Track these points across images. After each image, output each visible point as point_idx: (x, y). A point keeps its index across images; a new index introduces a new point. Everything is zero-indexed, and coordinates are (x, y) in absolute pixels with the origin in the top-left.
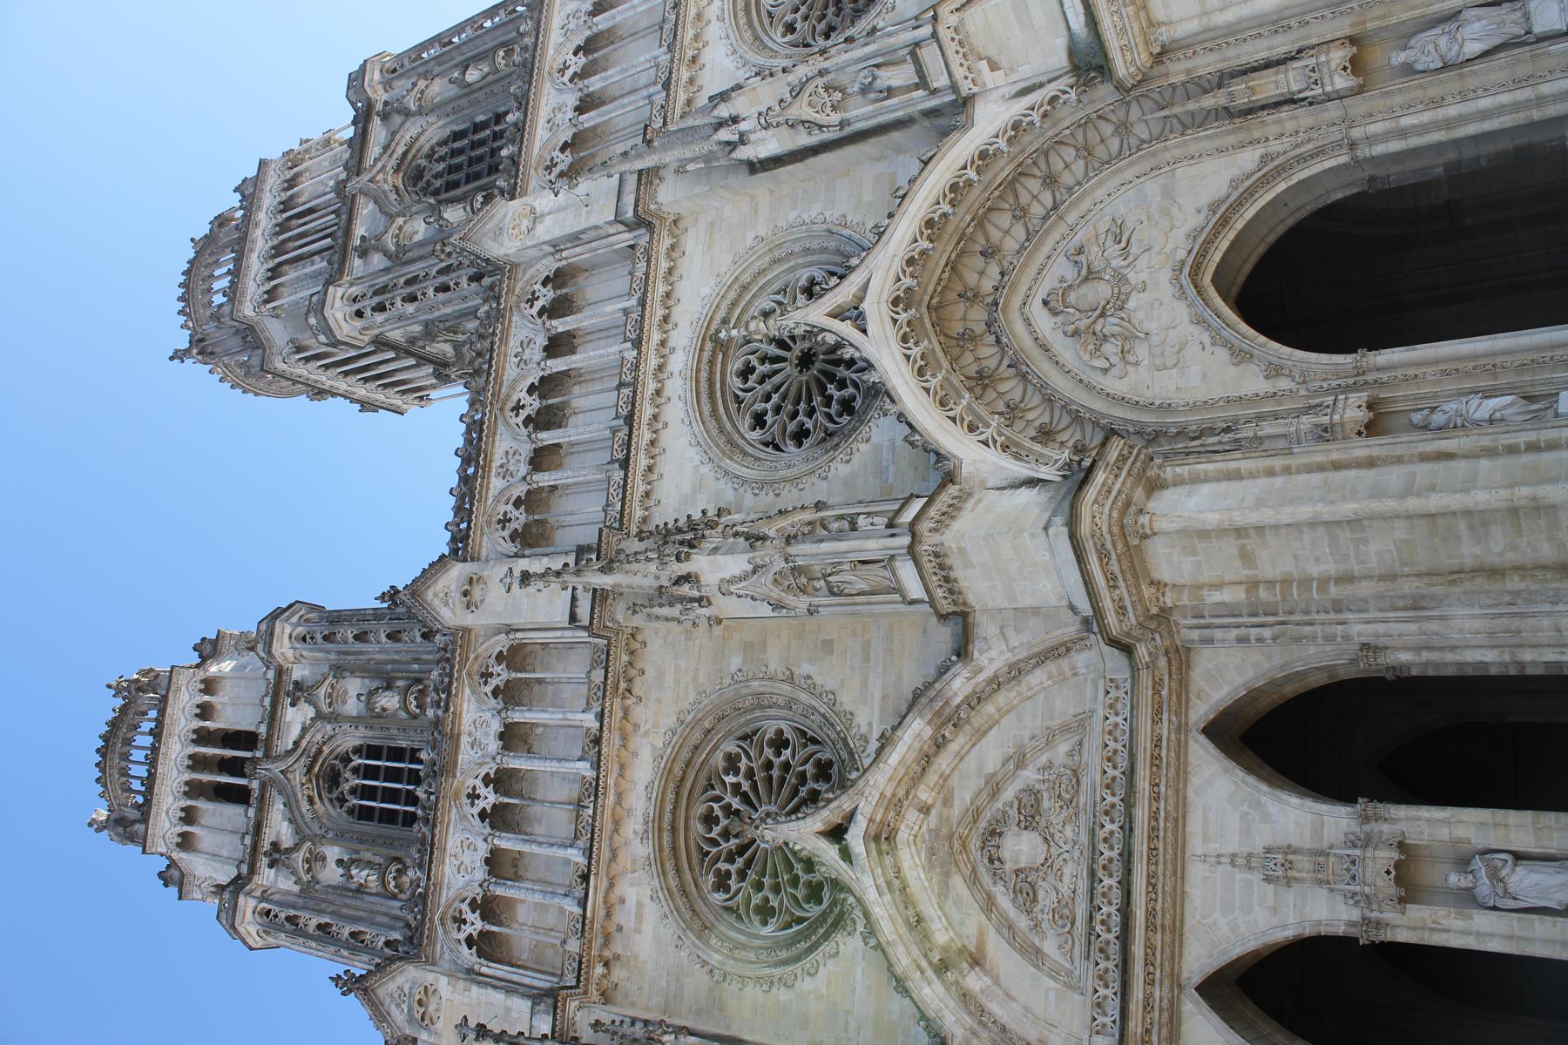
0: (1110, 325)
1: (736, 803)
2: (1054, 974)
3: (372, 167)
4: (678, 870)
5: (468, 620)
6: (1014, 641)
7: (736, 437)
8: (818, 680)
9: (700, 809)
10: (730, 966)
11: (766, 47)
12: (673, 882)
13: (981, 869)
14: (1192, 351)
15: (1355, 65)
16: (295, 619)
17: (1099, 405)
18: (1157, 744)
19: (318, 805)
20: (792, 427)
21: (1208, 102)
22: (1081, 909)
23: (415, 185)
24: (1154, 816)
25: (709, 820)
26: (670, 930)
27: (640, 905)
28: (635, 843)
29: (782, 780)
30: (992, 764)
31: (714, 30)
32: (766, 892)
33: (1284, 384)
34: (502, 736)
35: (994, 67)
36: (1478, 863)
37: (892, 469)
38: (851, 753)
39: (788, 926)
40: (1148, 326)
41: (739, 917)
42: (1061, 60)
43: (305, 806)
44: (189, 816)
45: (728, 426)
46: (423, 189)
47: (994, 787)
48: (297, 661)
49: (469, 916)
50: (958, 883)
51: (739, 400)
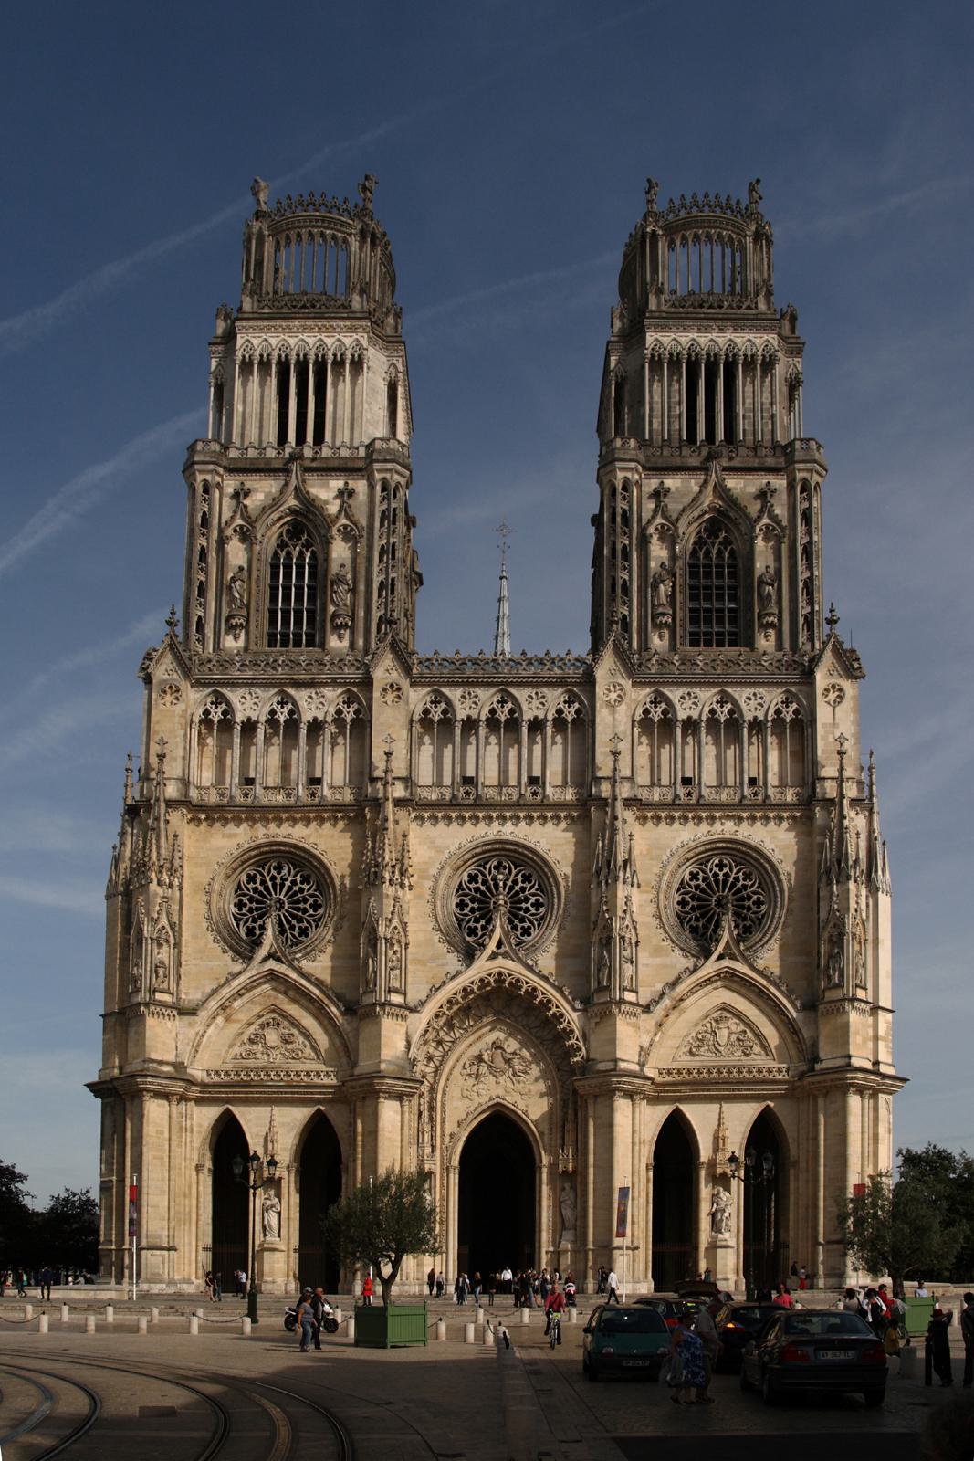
0: (484, 1069)
1: (288, 883)
2: (227, 1052)
6: (350, 1035)
7: (463, 868)
8: (341, 932)
10: (215, 895)
12: (246, 856)
13: (263, 1019)
15: (565, 1172)
16: (397, 477)
17: (450, 1063)
18: (312, 1093)
21: (570, 1112)
22: (251, 1063)
24: (286, 1093)
26: (227, 860)
27: (235, 835)
28: (263, 833)
31: (704, 827)
32: (249, 905)
34: (315, 719)
35: (597, 1023)
36: (277, 1200)
37: (434, 965)
39: (235, 918)
40: (481, 1086)
41: (236, 891)
42: (591, 1057)
43: (275, 516)
44: (265, 364)
45: (470, 862)
47: (296, 1024)
48: (371, 487)
49: (220, 710)
50: (257, 1009)
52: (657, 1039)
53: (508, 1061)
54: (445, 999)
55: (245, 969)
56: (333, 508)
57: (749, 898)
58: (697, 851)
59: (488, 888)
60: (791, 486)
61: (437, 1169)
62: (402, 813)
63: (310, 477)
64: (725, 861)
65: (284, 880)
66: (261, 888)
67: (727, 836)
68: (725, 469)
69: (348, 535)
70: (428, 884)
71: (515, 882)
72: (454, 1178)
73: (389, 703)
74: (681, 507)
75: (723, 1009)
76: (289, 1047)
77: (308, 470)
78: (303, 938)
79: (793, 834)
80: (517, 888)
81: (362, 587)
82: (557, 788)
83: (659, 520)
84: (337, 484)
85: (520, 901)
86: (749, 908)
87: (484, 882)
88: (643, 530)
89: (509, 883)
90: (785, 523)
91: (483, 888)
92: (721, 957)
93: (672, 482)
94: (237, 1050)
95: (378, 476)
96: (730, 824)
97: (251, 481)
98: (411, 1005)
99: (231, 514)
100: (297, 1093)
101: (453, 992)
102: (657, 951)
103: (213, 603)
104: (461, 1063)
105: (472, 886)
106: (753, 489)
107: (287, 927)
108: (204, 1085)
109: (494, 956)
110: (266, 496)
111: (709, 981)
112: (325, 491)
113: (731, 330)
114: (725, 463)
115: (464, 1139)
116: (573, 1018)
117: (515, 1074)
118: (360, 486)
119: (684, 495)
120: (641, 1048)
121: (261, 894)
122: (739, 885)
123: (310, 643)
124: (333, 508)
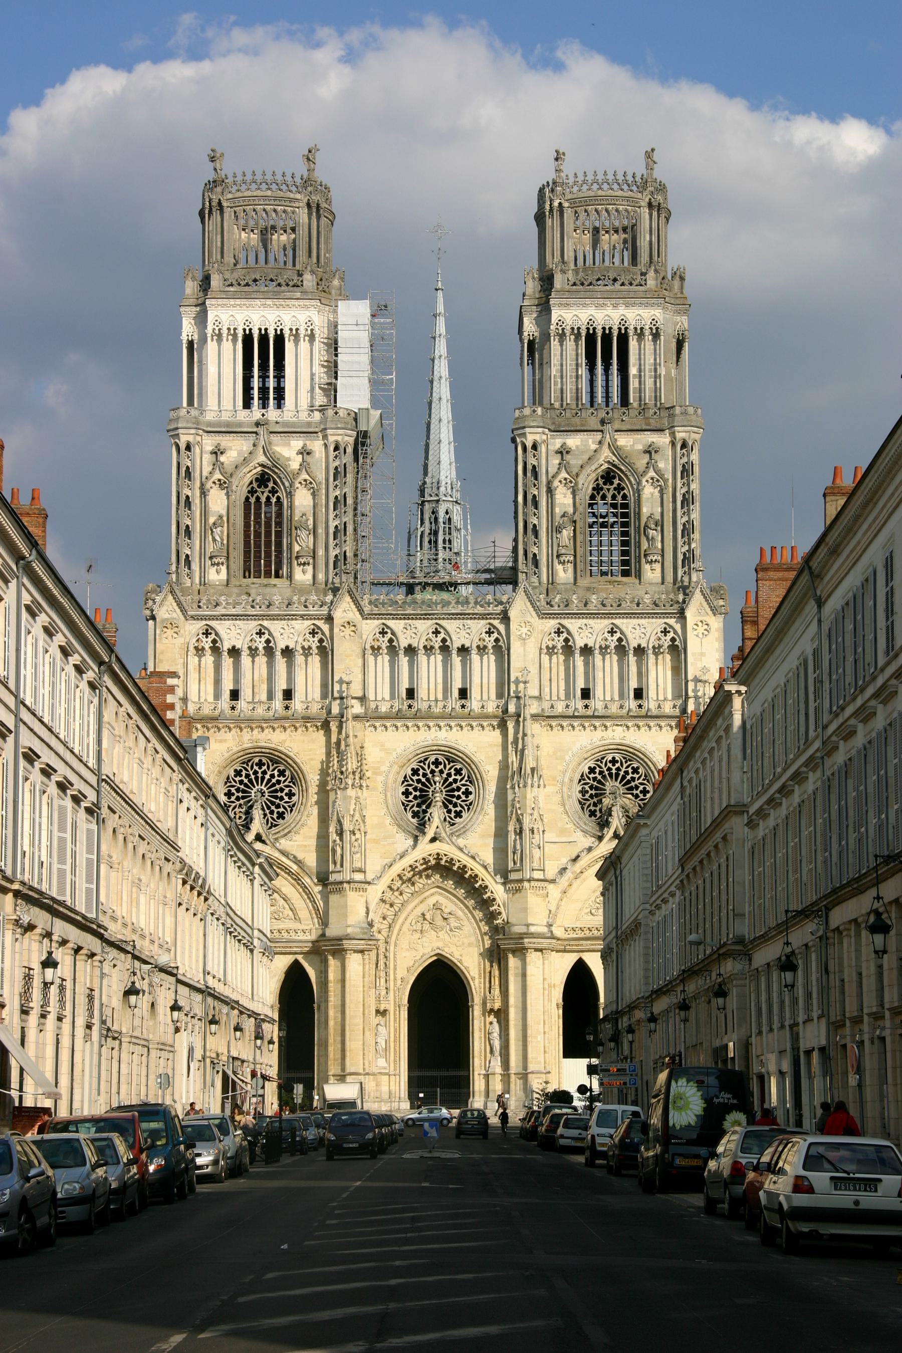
0: (427, 926)
1: (267, 777)
3: (617, 448)
5: (336, 630)
9: (264, 760)
12: (235, 756)
14: (414, 953)
19: (249, 475)
20: (411, 789)
23: (602, 477)
25: (260, 764)
28: (249, 739)
29: (276, 797)
30: (283, 889)
31: (599, 733)
33: (399, 982)
38: (286, 835)
51: (424, 762)
52: (563, 903)
54: (396, 874)
56: (295, 465)
59: (428, 780)
60: (673, 444)
61: (391, 1008)
62: (358, 725)
63: (275, 438)
65: (264, 773)
66: (246, 781)
67: (618, 741)
70: (380, 779)
71: (449, 775)
72: (404, 1014)
73: (347, 637)
74: (580, 462)
78: (281, 821)
80: (451, 780)
81: (321, 531)
82: (483, 695)
83: (564, 474)
84: (297, 443)
85: (453, 790)
87: (424, 775)
88: (549, 483)
89: (444, 776)
90: (669, 476)
91: (423, 780)
93: (573, 441)
95: (331, 439)
97: (225, 441)
98: (369, 880)
99: (210, 469)
102: (563, 832)
103: (198, 543)
104: (409, 921)
105: (415, 778)
106: (640, 447)
107: (267, 811)
109: (433, 840)
110: (240, 452)
112: (288, 451)
114: (617, 426)
115: (411, 982)
116: (497, 890)
117: (451, 930)
118: (317, 446)
119: (583, 452)
121: (246, 785)
122: (628, 777)
123: (277, 576)
124: (295, 465)
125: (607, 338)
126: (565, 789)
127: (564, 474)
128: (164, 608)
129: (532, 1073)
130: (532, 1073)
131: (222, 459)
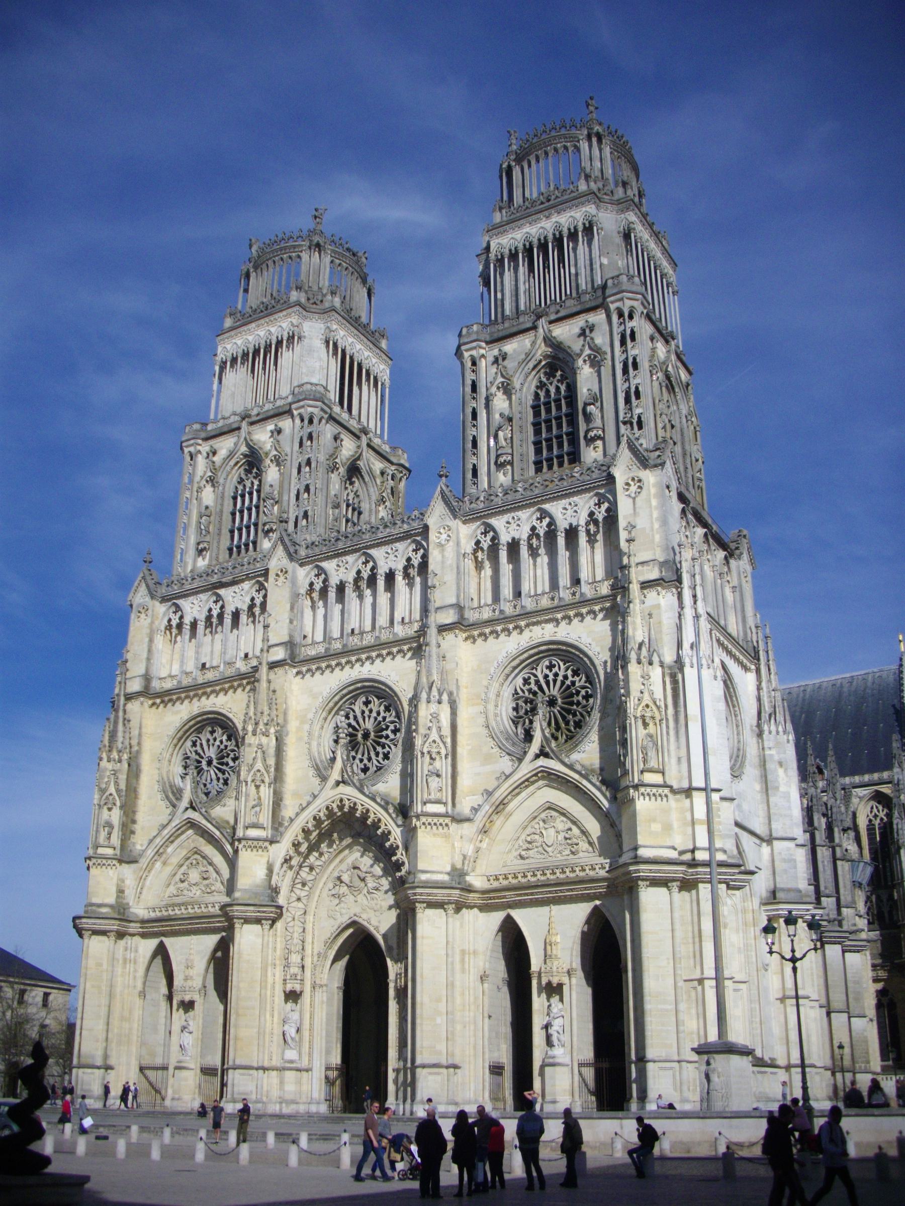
0: (344, 889)
4: (194, 725)
11: (508, 676)
26: (171, 731)
33: (316, 959)
40: (342, 905)
43: (232, 463)
46: (541, 382)
52: (484, 845)
53: (363, 880)
55: (170, 821)
56: (268, 447)
57: (578, 693)
58: (522, 658)
64: (554, 662)
65: (215, 739)
68: (551, 322)
69: (278, 461)
75: (549, 808)
76: (207, 882)
77: (252, 423)
79: (608, 622)
86: (578, 703)
92: (537, 756)
93: (510, 347)
94: (172, 890)
95: (295, 413)
96: (549, 627)
97: (216, 443)
100: (204, 923)
101: (305, 821)
108: (143, 922)
111: (527, 782)
113: (556, 215)
118: (286, 424)
120: (465, 857)
122: (568, 682)
124: (268, 447)
125: (543, 247)
126: (491, 707)
127: (501, 379)
128: (139, 595)
129: (424, 1066)
130: (424, 1066)
131: (215, 459)
